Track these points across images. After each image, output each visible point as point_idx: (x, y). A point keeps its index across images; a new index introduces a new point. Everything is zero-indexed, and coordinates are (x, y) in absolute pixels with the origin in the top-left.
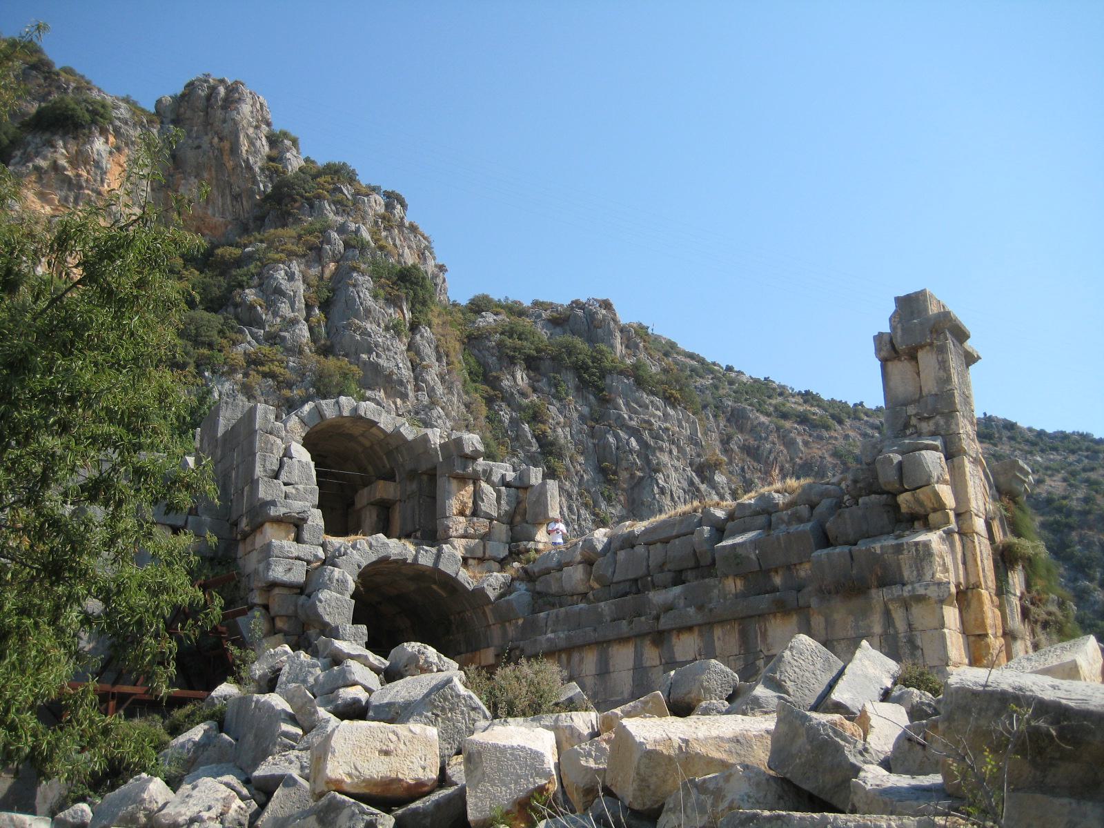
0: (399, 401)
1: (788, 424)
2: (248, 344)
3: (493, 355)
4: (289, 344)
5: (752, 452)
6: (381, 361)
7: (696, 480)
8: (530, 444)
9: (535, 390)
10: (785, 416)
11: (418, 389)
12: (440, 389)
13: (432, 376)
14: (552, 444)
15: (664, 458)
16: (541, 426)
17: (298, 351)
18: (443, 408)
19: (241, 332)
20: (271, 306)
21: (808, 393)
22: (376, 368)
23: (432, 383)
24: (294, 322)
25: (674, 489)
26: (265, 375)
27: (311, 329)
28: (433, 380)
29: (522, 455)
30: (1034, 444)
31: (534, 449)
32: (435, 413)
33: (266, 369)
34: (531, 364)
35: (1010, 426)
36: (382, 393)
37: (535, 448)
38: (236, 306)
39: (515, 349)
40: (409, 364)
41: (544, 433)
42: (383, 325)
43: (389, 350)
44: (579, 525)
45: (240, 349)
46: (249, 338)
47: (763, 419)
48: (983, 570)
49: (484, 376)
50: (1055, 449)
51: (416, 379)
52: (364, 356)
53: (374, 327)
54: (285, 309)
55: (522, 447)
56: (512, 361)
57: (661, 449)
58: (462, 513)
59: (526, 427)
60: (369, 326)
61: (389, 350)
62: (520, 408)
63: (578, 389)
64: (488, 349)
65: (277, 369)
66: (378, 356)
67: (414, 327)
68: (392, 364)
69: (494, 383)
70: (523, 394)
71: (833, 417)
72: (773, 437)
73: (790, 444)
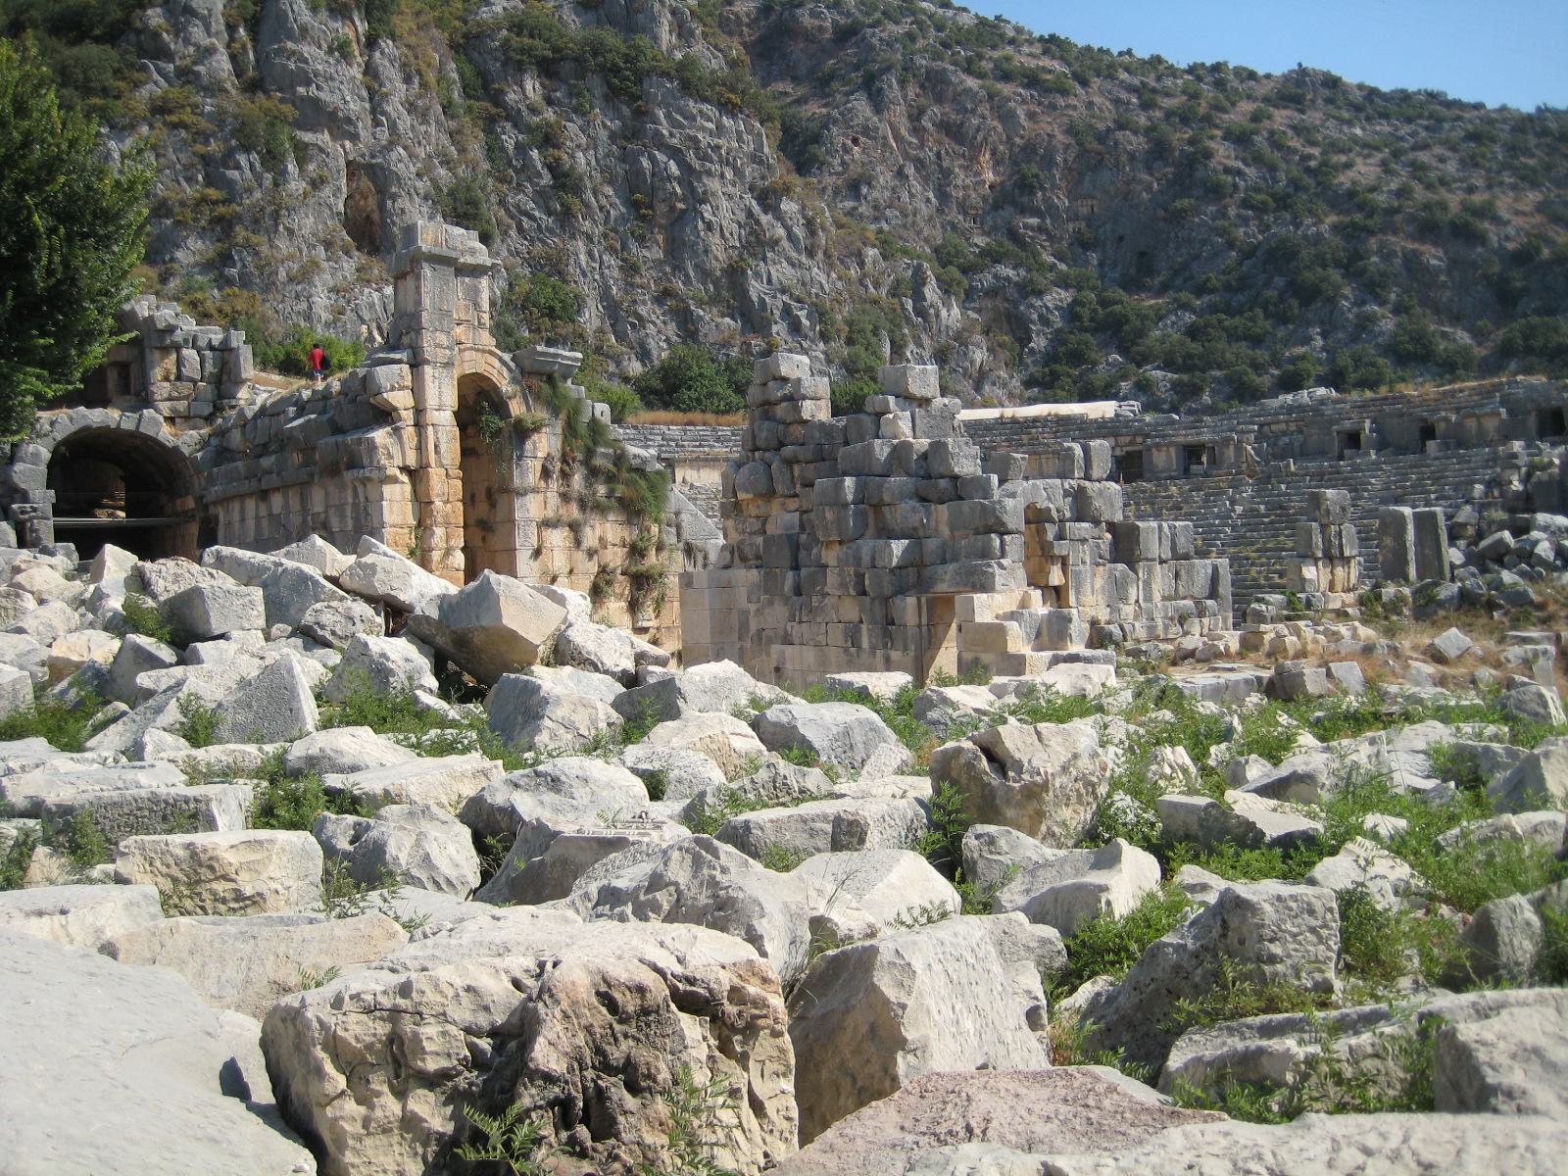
0: (348, 144)
1: (1006, 89)
2: (155, 86)
3: (496, 59)
4: (205, 80)
5: (952, 131)
6: (322, 95)
7: (756, 208)
8: (539, 175)
9: (549, 102)
10: (1006, 76)
11: (377, 123)
12: (405, 121)
13: (394, 107)
14: (566, 175)
15: (714, 185)
16: (556, 152)
17: (215, 89)
19: (144, 68)
20: (178, 30)
21: (1053, 39)
22: (316, 103)
23: (394, 115)
24: (210, 51)
25: (725, 224)
26: (175, 126)
27: (233, 58)
28: (396, 110)
29: (529, 189)
30: (1358, 108)
31: (543, 182)
32: (394, 156)
33: (174, 118)
34: (547, 69)
35: (1332, 82)
36: (326, 136)
37: (546, 179)
38: (139, 32)
39: (522, 51)
40: (365, 94)
41: (558, 160)
42: (325, 46)
43: (332, 79)
44: (602, 274)
45: (144, 92)
46: (156, 76)
47: (972, 83)
48: (437, 452)
49: (484, 88)
50: (1385, 116)
51: (373, 111)
52: (301, 90)
53: (313, 49)
54: (197, 32)
55: (529, 180)
56: (520, 68)
57: (709, 173)
58: (166, 379)
59: (535, 154)
60: (307, 50)
61: (332, 79)
62: (529, 129)
63: (607, 98)
64: (490, 51)
65: (187, 117)
66: (318, 88)
67: (371, 43)
69: (497, 98)
70: (534, 110)
71: (1076, 76)
72: (984, 109)
73: (1007, 118)
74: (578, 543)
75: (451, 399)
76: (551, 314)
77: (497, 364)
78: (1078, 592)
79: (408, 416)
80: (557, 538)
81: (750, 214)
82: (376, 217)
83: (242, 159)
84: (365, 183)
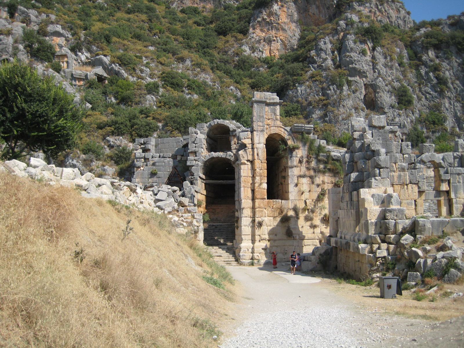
0: (364, 79)
2: (312, 71)
3: (420, 47)
4: (324, 67)
6: (356, 66)
8: (433, 81)
9: (437, 57)
11: (375, 72)
12: (383, 71)
13: (380, 66)
14: (441, 79)
16: (438, 73)
17: (327, 69)
18: (382, 78)
19: (309, 67)
20: (318, 55)
22: (354, 69)
23: (379, 69)
24: (326, 59)
26: (316, 81)
27: (333, 60)
28: (380, 67)
29: (429, 85)
31: (433, 83)
32: (378, 81)
33: (314, 79)
34: (437, 47)
36: (358, 78)
37: (435, 81)
38: (309, 58)
39: (427, 43)
40: (371, 64)
41: (438, 75)
42: (358, 52)
43: (359, 61)
44: (454, 109)
45: (309, 73)
46: (312, 69)
48: (258, 154)
49: (416, 57)
51: (373, 69)
52: (351, 66)
53: (355, 54)
54: (323, 55)
55: (429, 82)
56: (427, 49)
58: (235, 144)
59: (431, 74)
60: (352, 54)
61: (359, 61)
62: (429, 67)
63: (457, 53)
64: (418, 45)
65: (318, 78)
66: (356, 64)
67: (374, 49)
68: (360, 67)
69: (420, 59)
70: (431, 61)
74: (313, 183)
75: (263, 140)
76: (434, 123)
77: (283, 130)
78: (456, 193)
79: (249, 146)
80: (305, 181)
81: (58, 69)
82: (374, 99)
83: (331, 87)
84: (371, 90)
